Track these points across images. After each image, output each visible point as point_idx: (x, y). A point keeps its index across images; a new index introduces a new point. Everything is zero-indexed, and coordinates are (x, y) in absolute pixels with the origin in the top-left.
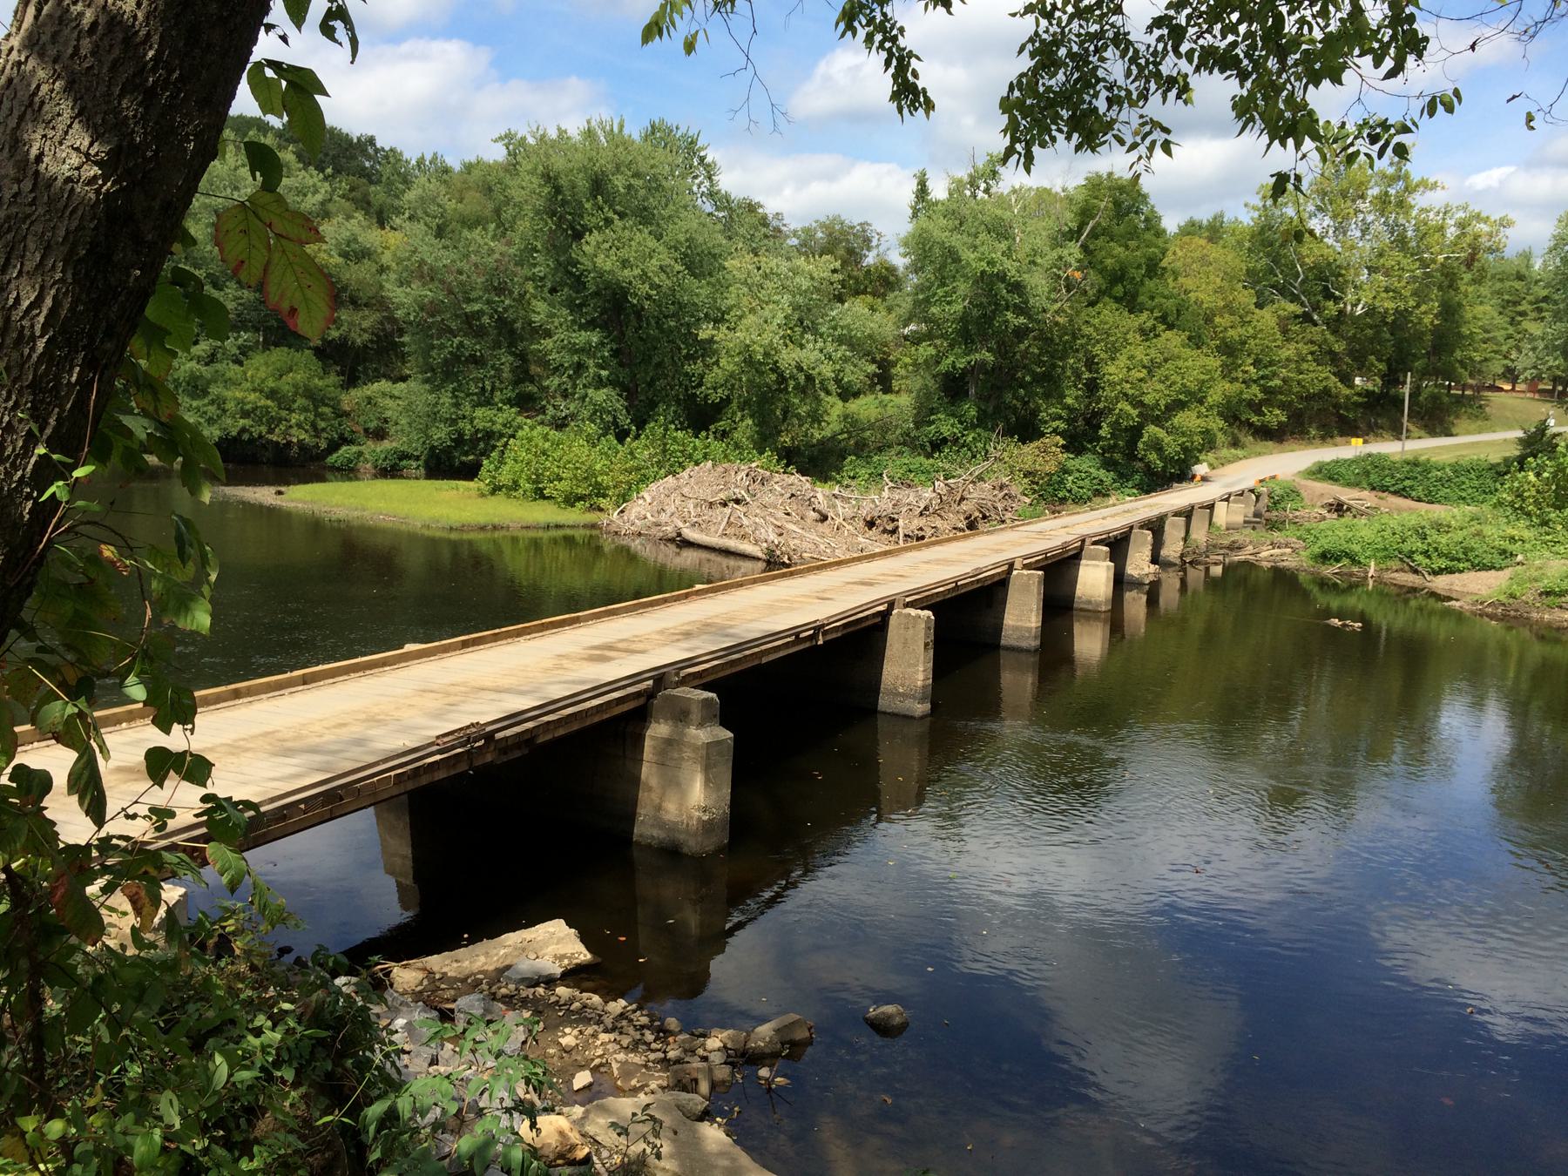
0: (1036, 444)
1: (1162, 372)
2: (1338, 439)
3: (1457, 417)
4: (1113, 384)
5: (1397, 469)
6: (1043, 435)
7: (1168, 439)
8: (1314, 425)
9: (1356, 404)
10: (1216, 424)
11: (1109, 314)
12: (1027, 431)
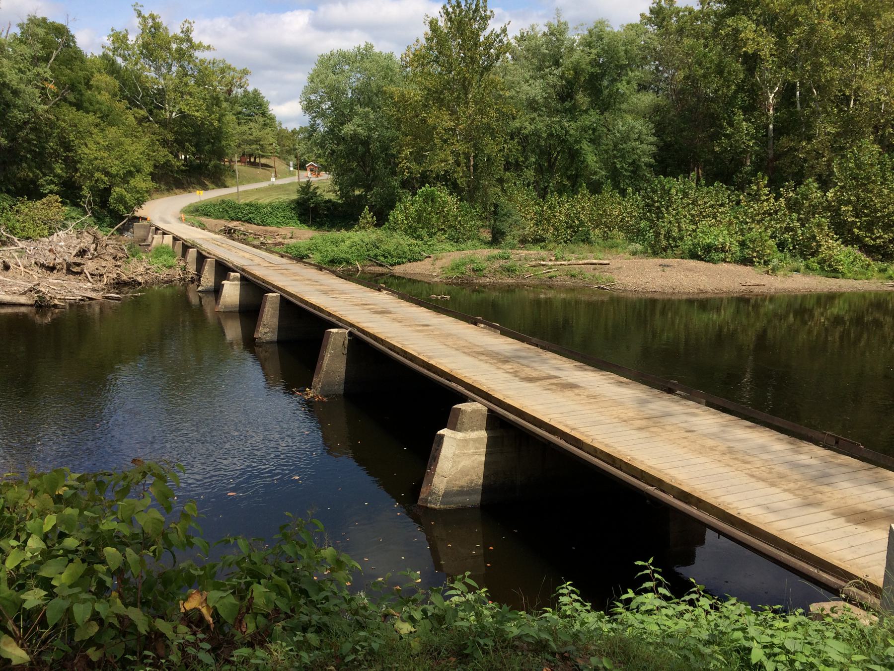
0: (44, 200)
1: (116, 153)
3: (226, 177)
4: (90, 162)
5: (243, 208)
6: (45, 195)
8: (163, 183)
9: (182, 171)
10: (151, 184)
11: (70, 114)
12: (33, 192)
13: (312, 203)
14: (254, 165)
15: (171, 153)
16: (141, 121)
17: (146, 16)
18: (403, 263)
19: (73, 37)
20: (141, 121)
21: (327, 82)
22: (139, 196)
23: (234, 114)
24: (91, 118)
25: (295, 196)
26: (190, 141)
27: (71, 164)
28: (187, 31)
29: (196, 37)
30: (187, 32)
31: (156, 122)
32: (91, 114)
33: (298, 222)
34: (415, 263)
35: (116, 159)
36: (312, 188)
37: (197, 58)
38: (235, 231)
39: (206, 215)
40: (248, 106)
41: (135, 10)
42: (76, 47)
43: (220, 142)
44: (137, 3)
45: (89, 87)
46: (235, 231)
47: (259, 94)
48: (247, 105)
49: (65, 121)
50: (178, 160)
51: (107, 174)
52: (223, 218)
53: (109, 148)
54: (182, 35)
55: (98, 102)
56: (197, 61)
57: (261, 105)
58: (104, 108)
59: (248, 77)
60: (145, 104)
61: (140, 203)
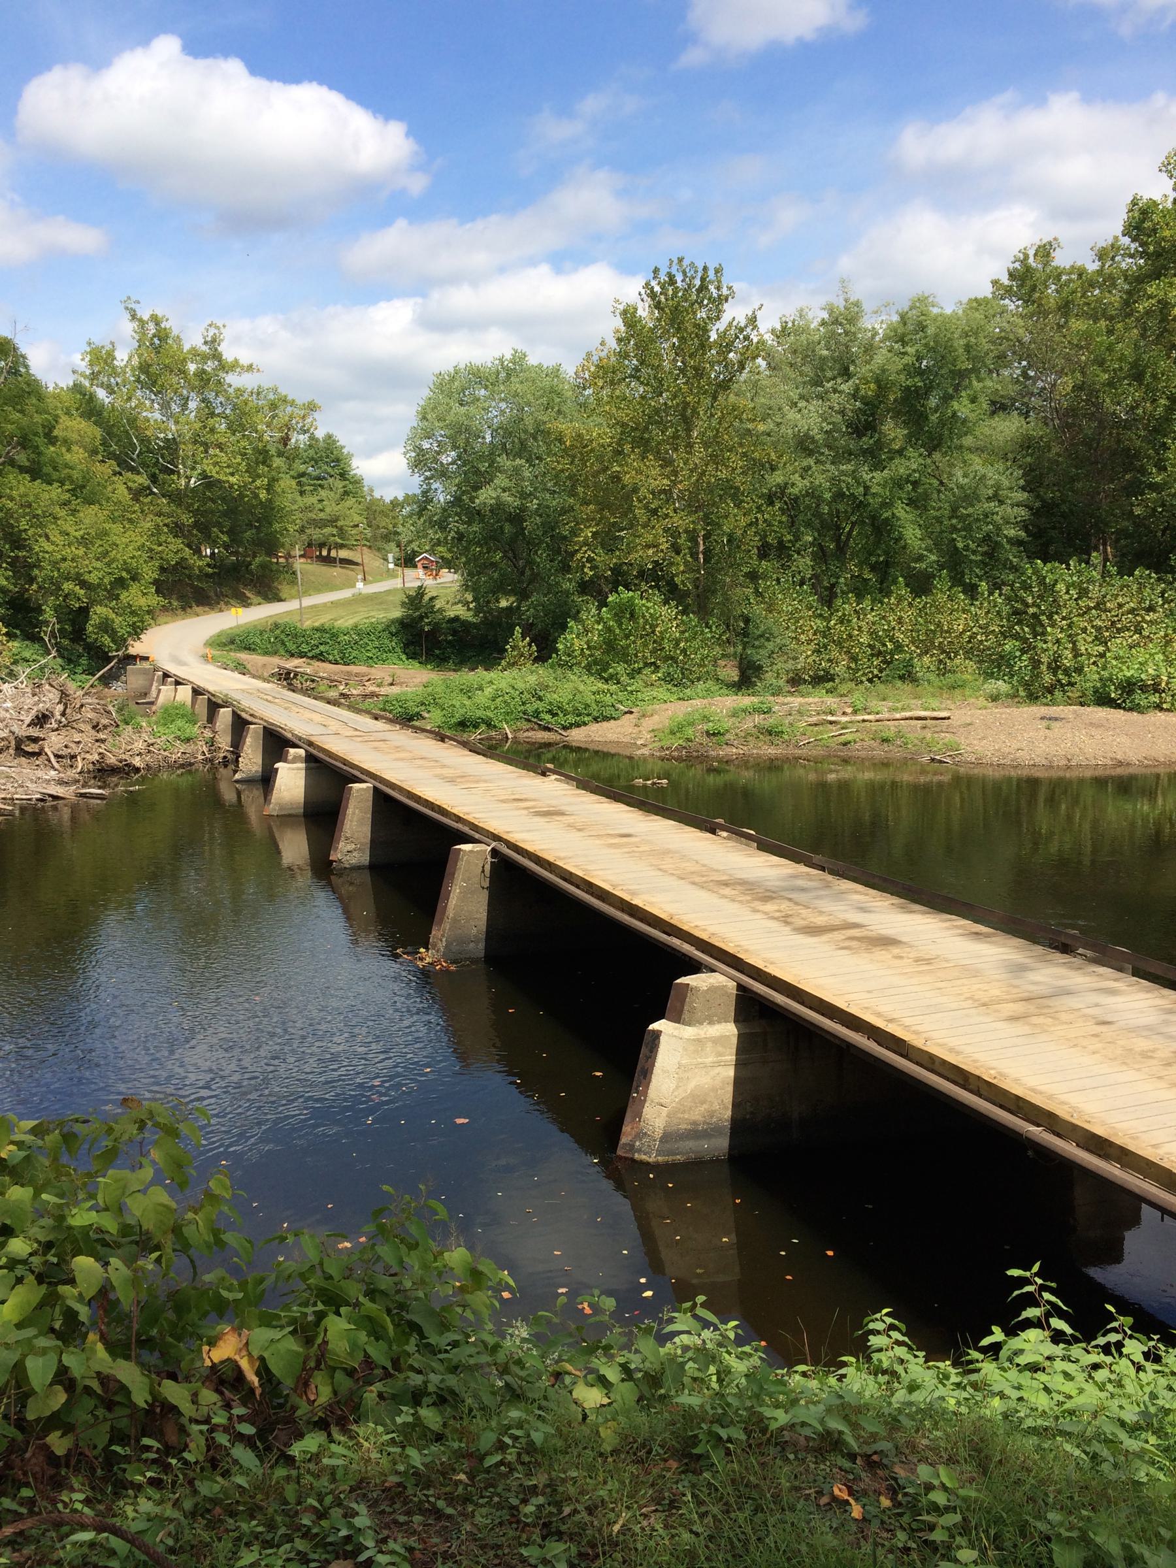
1: (96, 549)
2: (199, 609)
3: (280, 583)
4: (55, 564)
5: (309, 636)
7: (118, 620)
8: (174, 596)
9: (207, 575)
10: (154, 600)
13: (429, 624)
14: (328, 561)
15: (189, 546)
16: (137, 494)
17: (146, 318)
18: (585, 724)
19: (24, 357)
20: (137, 494)
21: (450, 418)
22: (135, 619)
23: (293, 477)
24: (55, 492)
25: (397, 613)
26: (219, 525)
27: (23, 570)
28: (214, 341)
29: (228, 352)
30: (213, 342)
31: (164, 496)
32: (56, 485)
33: (404, 657)
34: (605, 724)
35: (98, 559)
36: (426, 598)
37: (230, 386)
38: (296, 675)
39: (249, 648)
40: (316, 463)
41: (127, 308)
42: (30, 375)
43: (271, 524)
44: (129, 298)
45: (52, 440)
46: (296, 675)
47: (335, 442)
48: (315, 461)
49: (12, 499)
50: (201, 557)
51: (83, 584)
52: (275, 653)
53: (84, 541)
54: (205, 348)
55: (67, 466)
56: (231, 390)
57: (338, 460)
58: (76, 474)
59: (316, 415)
60: (144, 465)
61: (137, 631)
